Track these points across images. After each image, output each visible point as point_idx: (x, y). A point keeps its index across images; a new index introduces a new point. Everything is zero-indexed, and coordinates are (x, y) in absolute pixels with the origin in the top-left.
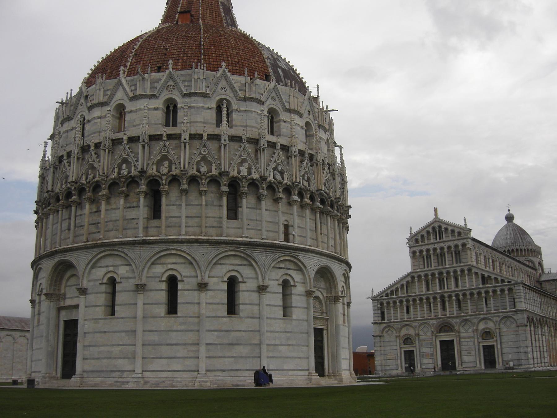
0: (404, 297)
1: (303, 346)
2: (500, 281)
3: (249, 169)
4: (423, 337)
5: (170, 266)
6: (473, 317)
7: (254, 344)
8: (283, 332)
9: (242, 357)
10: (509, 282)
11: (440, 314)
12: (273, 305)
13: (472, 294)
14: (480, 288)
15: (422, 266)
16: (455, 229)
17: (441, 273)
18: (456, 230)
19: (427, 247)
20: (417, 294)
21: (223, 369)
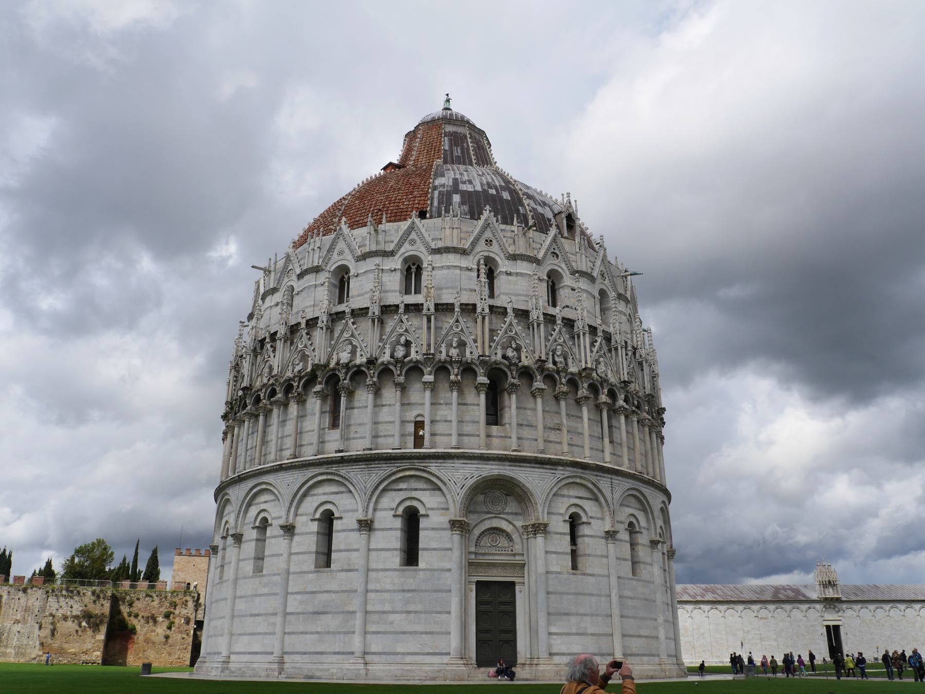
1: (440, 613)
3: (353, 353)
5: (263, 507)
7: (348, 612)
8: (399, 591)
9: (329, 633)
12: (382, 550)
21: (303, 650)
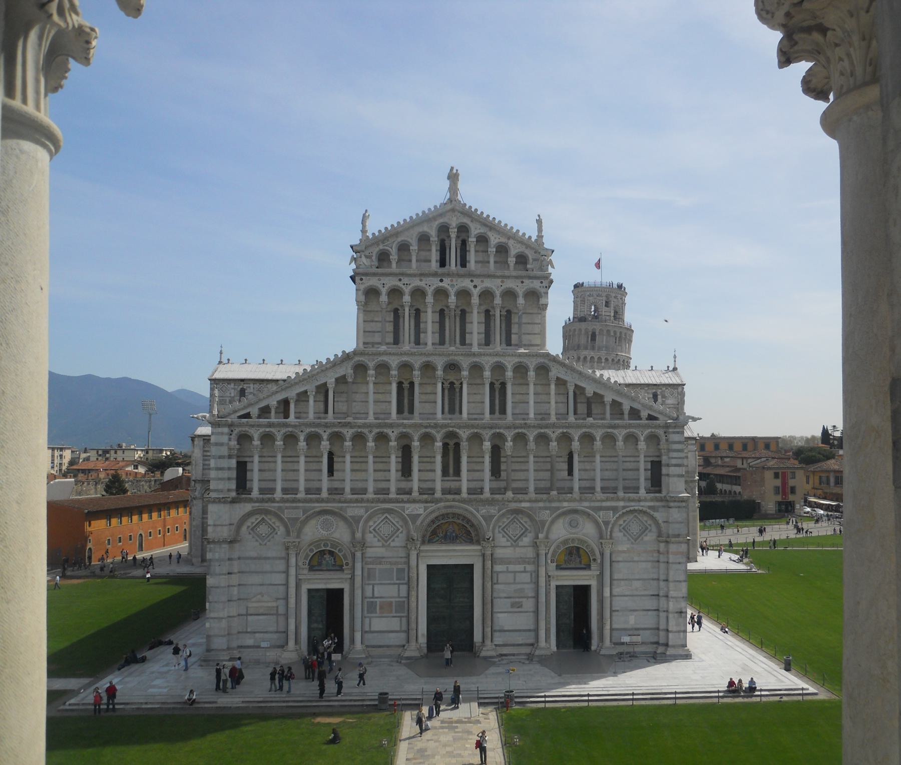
0: (326, 426)
2: (626, 412)
4: (375, 550)
6: (541, 504)
10: (651, 418)
11: (438, 486)
13: (543, 439)
14: (570, 426)
15: (390, 338)
16: (511, 243)
17: (452, 367)
18: (515, 249)
19: (416, 282)
20: (371, 419)
